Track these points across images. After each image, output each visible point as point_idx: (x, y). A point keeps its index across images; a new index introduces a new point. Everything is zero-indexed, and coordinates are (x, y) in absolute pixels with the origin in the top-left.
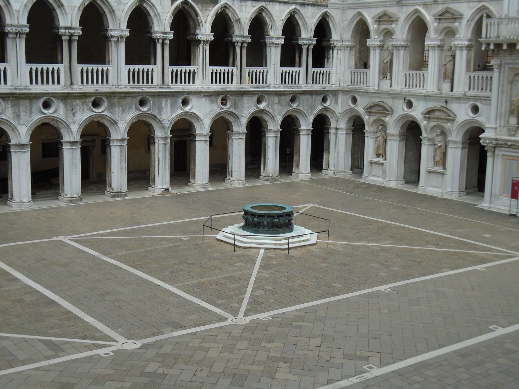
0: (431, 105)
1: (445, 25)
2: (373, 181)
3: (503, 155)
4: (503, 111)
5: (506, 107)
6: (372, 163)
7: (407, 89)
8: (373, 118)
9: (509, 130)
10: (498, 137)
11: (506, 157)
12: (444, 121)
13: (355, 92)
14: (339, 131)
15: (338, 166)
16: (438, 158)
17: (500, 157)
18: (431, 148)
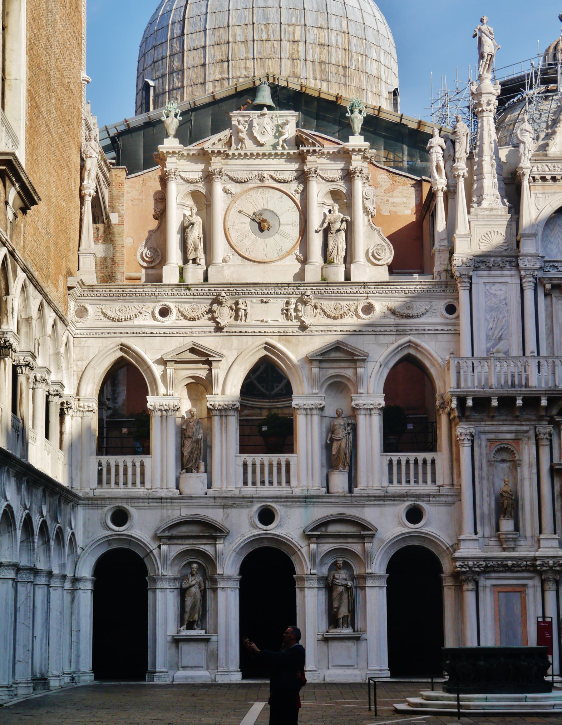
0: (319, 513)
1: (332, 372)
2: (187, 678)
3: (494, 586)
4: (486, 511)
5: (490, 505)
6: (177, 641)
7: (249, 490)
8: (176, 549)
9: (500, 542)
10: (488, 555)
11: (500, 589)
12: (350, 540)
13: (127, 499)
14: (81, 585)
15: (78, 662)
16: (344, 611)
17: (488, 590)
18: (322, 596)
